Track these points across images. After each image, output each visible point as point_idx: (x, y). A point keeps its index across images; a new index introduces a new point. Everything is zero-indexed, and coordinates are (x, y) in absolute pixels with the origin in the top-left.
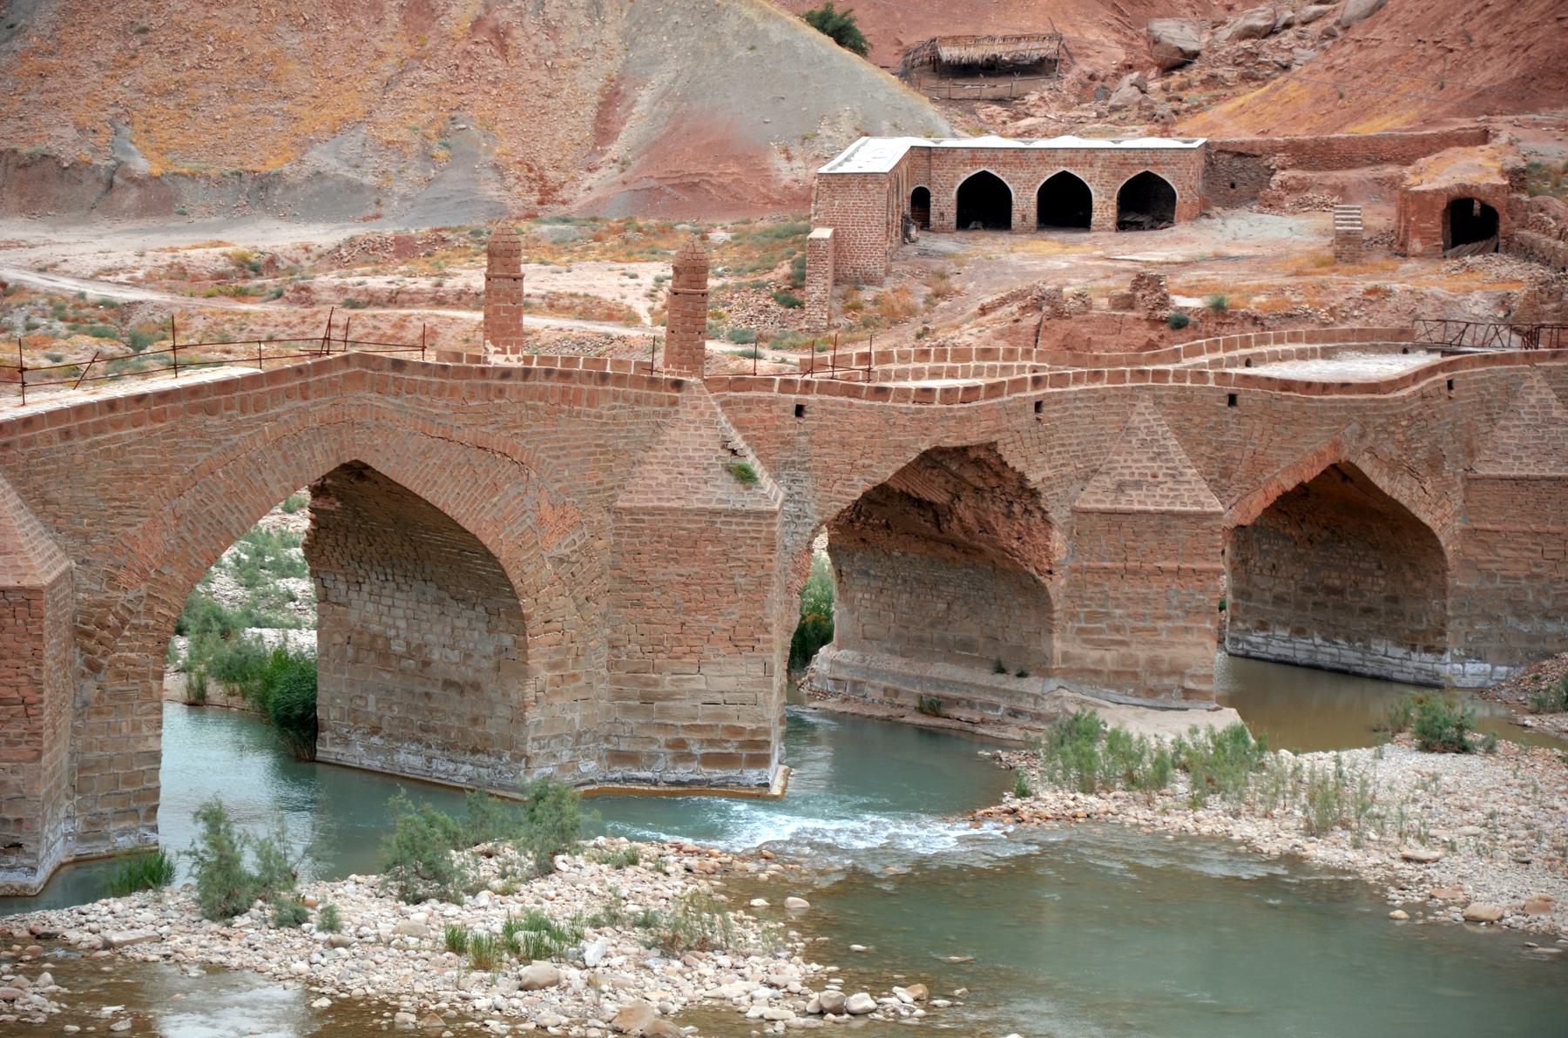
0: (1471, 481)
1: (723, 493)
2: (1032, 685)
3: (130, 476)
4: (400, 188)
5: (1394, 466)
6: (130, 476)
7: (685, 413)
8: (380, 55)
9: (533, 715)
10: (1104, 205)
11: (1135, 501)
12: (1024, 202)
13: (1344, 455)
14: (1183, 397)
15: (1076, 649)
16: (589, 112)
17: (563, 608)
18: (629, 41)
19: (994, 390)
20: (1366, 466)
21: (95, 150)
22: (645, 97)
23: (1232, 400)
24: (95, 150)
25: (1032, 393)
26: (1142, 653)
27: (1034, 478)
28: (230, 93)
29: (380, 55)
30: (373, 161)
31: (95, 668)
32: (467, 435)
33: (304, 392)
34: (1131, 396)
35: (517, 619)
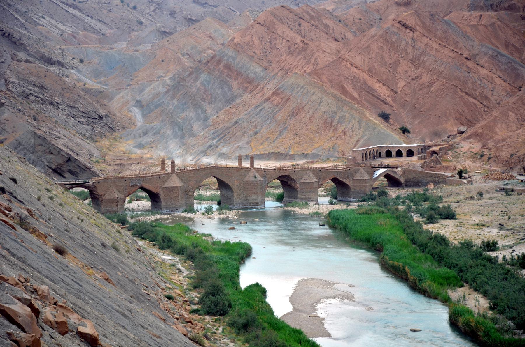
0: (353, 180)
1: (254, 179)
2: (297, 200)
3: (190, 177)
4: (324, 155)
5: (342, 178)
6: (190, 177)
7: (251, 172)
8: (328, 136)
9: (235, 201)
10: (404, 154)
11: (306, 181)
12: (394, 153)
13: (335, 177)
14: (314, 171)
15: (301, 196)
16: (354, 143)
17: (238, 190)
18: (363, 133)
19: (289, 169)
20: (339, 178)
21: (285, 151)
22: (362, 140)
23: (320, 171)
24: (285, 151)
25: (294, 170)
26: (307, 196)
27: (294, 178)
28: (306, 143)
29: (328, 136)
30: (322, 151)
31: (187, 195)
32: (226, 174)
33: (208, 169)
34: (307, 170)
35: (232, 191)
